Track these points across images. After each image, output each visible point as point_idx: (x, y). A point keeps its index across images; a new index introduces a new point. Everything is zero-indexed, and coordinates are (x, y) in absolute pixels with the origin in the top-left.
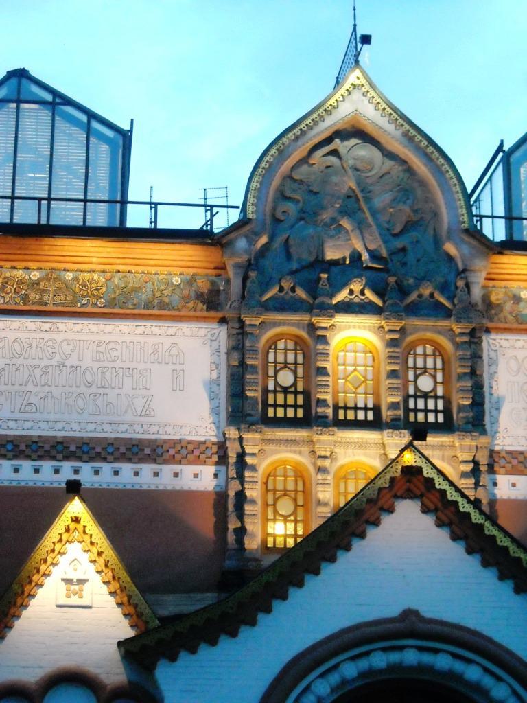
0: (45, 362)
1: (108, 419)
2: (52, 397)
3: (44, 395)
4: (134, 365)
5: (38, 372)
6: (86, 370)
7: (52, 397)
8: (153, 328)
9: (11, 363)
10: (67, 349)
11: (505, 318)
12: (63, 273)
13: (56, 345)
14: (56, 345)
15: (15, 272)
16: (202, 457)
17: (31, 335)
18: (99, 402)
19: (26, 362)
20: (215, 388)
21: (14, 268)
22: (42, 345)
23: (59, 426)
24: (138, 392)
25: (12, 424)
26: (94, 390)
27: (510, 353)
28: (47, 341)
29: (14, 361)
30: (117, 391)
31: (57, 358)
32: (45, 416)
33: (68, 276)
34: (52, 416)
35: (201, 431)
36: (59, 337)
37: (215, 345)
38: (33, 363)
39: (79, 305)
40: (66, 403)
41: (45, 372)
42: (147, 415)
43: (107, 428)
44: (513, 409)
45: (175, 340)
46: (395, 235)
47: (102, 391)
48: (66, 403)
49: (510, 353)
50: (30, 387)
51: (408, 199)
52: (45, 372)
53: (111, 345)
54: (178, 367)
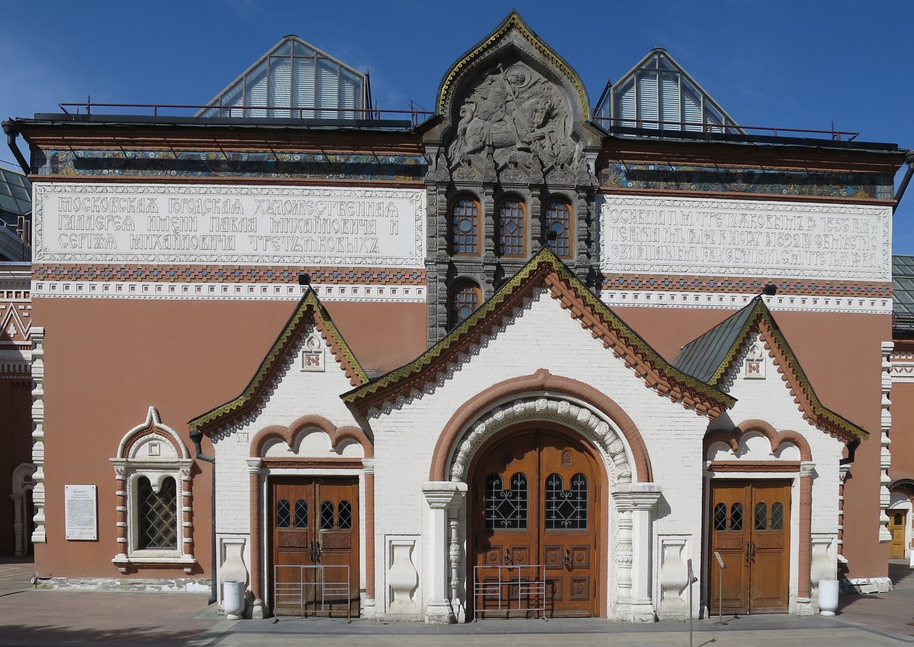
0: (306, 217)
1: (350, 254)
2: (312, 240)
3: (305, 239)
4: (366, 218)
5: (302, 223)
6: (334, 221)
7: (312, 240)
8: (377, 193)
9: (284, 217)
10: (320, 208)
11: (611, 183)
12: (316, 156)
13: (313, 205)
14: (313, 205)
15: (284, 155)
16: (411, 279)
17: (296, 199)
18: (343, 243)
19: (294, 217)
20: (419, 233)
21: (283, 153)
22: (304, 206)
23: (317, 260)
24: (368, 236)
25: (286, 259)
26: (339, 235)
27: (612, 208)
28: (308, 202)
29: (286, 216)
30: (356, 236)
31: (315, 214)
32: (309, 253)
33: (320, 158)
34: (313, 253)
35: (410, 261)
36: (315, 200)
37: (419, 204)
38: (299, 217)
39: (327, 177)
40: (321, 245)
41: (307, 223)
42: (374, 251)
43: (348, 260)
44: (613, 245)
45: (391, 200)
46: (539, 127)
47: (345, 235)
48: (321, 245)
49: (612, 208)
50: (298, 234)
51: (548, 102)
52: (307, 223)
53: (350, 205)
54: (395, 219)
